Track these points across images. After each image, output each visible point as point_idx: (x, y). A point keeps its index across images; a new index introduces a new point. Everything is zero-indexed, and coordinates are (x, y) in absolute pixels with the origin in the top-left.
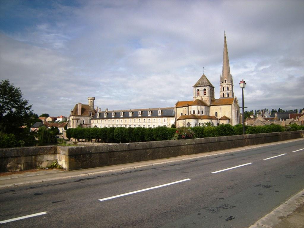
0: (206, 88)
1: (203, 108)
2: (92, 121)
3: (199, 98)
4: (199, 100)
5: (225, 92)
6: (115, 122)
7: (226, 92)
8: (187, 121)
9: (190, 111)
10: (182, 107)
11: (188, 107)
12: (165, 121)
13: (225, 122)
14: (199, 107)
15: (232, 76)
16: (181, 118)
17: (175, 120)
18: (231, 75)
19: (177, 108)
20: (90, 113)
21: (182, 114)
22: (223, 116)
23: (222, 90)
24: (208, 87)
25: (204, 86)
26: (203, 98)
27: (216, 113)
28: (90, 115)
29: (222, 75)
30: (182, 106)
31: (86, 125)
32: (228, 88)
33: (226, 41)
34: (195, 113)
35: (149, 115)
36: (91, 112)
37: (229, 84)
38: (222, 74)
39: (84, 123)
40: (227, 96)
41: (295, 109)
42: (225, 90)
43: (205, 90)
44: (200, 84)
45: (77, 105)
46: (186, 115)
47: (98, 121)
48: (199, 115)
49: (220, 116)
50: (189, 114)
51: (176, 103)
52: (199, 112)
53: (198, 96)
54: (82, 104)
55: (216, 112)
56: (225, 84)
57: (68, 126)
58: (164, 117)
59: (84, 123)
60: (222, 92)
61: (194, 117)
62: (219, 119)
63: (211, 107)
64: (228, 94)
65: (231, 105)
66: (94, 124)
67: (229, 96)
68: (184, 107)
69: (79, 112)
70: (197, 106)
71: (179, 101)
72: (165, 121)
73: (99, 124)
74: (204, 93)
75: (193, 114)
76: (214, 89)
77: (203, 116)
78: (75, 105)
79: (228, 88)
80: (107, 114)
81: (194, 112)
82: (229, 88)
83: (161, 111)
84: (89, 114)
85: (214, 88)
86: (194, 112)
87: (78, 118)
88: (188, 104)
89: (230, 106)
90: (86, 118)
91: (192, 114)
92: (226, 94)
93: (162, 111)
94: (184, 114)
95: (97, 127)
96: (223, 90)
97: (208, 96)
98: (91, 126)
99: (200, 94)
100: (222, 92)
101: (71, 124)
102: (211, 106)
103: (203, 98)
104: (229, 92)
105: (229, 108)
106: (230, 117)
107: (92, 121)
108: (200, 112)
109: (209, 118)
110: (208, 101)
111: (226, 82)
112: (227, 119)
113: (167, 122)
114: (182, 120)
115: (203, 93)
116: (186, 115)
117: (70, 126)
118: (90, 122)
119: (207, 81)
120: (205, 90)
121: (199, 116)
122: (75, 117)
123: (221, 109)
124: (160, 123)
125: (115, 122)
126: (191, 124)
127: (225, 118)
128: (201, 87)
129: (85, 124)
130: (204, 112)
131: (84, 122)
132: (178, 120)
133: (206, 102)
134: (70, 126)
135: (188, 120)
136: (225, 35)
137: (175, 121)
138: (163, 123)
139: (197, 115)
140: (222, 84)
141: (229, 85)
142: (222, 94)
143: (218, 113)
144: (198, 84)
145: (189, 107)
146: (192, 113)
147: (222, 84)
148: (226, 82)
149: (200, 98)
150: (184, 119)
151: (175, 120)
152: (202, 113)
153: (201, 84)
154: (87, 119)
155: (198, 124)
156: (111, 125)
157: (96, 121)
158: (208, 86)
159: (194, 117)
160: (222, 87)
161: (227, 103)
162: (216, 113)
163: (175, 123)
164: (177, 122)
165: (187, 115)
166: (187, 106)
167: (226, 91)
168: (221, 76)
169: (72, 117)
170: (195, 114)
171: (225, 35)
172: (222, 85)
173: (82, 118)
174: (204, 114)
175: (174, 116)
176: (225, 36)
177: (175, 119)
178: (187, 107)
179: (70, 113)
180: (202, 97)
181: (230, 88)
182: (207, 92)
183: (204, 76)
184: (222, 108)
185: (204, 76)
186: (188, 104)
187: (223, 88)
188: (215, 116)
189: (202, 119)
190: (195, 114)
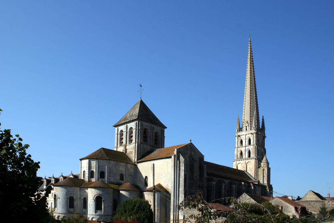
5: (243, 149)
14: (94, 163)
32: (250, 140)
52: (91, 174)
67: (251, 155)
75: (83, 178)
76: (165, 130)
79: (250, 140)
82: (252, 141)
102: (138, 163)
104: (252, 147)
105: (168, 166)
108: (96, 175)
111: (246, 129)
140: (240, 133)
141: (252, 134)
148: (246, 129)
172: (239, 136)
181: (253, 141)
187: (241, 142)
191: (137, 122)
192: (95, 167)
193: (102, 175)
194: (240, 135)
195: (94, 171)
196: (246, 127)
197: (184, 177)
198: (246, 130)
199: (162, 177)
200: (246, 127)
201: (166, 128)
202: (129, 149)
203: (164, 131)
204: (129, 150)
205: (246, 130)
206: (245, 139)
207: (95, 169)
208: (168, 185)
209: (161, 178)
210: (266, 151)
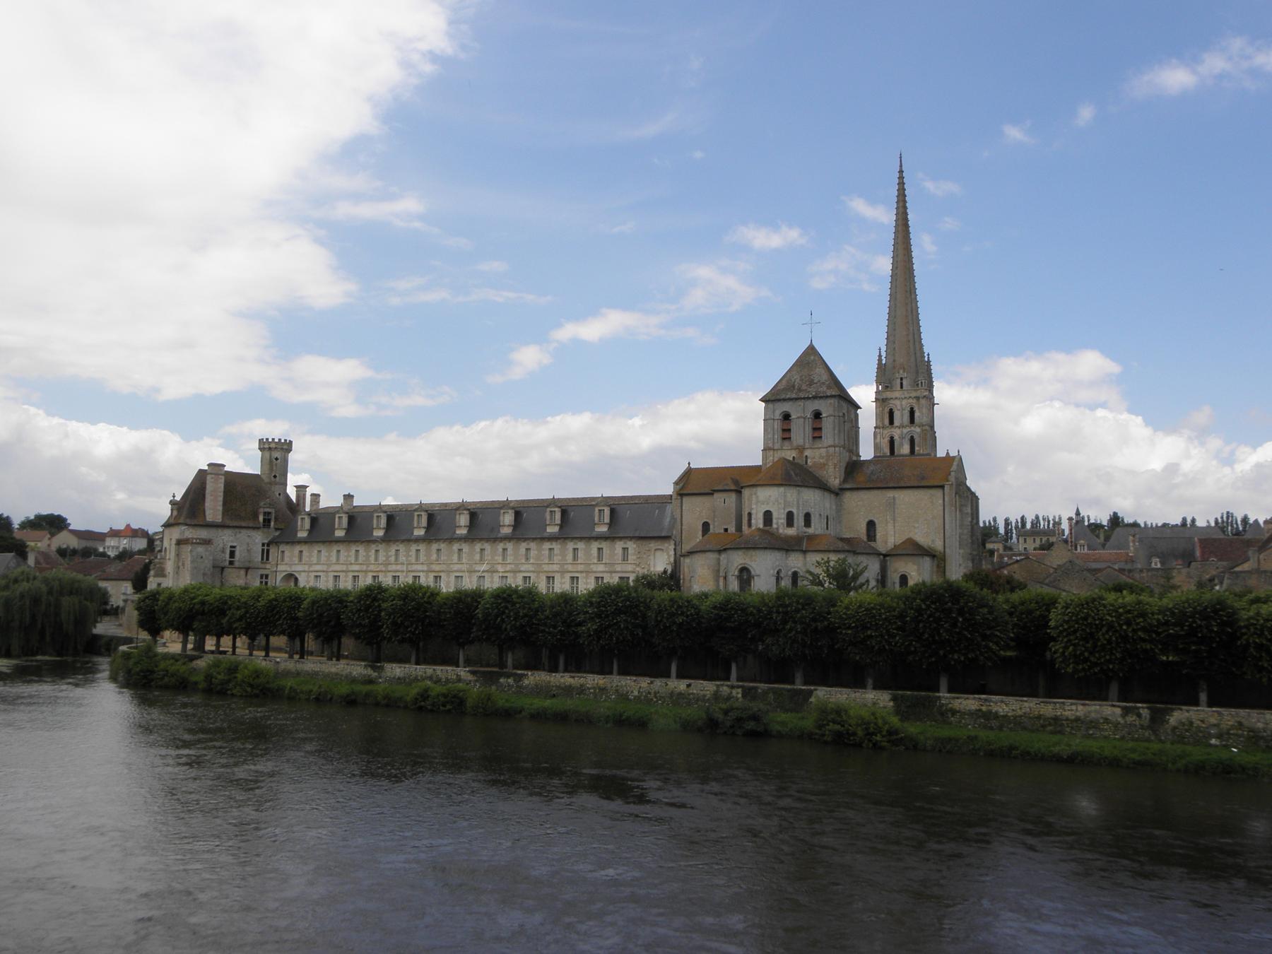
0: (826, 408)
1: (811, 499)
2: (273, 550)
3: (790, 455)
4: (789, 461)
5: (896, 433)
6: (388, 557)
7: (905, 431)
8: (737, 560)
9: (750, 514)
10: (711, 494)
11: (739, 492)
12: (625, 558)
13: (918, 573)
14: (791, 494)
15: (929, 361)
16: (708, 547)
17: (672, 553)
18: (925, 355)
19: (685, 499)
20: (265, 513)
21: (706, 527)
22: (907, 537)
23: (887, 422)
24: (831, 401)
25: (815, 397)
26: (807, 453)
27: (871, 525)
28: (267, 522)
29: (884, 354)
30: (707, 491)
31: (243, 572)
32: (912, 412)
33: (905, 202)
34: (774, 521)
35: (553, 530)
36: (272, 511)
37: (918, 394)
38: (884, 349)
39: (231, 563)
40: (906, 449)
41: (1216, 519)
42: (897, 423)
43: (817, 415)
44: (793, 386)
45: (201, 475)
46: (726, 530)
47: (305, 554)
48: (791, 532)
49: (889, 537)
50: (745, 527)
51: (676, 477)
52: (790, 518)
53: (786, 443)
54: (226, 469)
55: (872, 519)
56: (897, 394)
57: (152, 573)
58: (621, 538)
59: (231, 563)
60: (887, 432)
61: (771, 541)
62: (885, 556)
63: (848, 495)
64: (912, 441)
65: (942, 487)
66: (281, 568)
67: (917, 448)
68: (716, 495)
69: (213, 508)
70: (782, 489)
71: (692, 466)
72: (625, 558)
73: (306, 568)
74: (815, 429)
75: (765, 524)
76: (859, 411)
77: (811, 538)
78: (189, 478)
79: (912, 412)
80: (351, 519)
81: (768, 516)
82: (917, 414)
83: (607, 511)
84: (261, 518)
85: (859, 407)
86: (768, 516)
87: (203, 534)
88: (736, 482)
89: (938, 493)
90: (244, 534)
91: (761, 526)
92: (902, 438)
93: (613, 512)
94: (716, 529)
95: (296, 579)
96: (891, 422)
97: (830, 442)
98: (267, 576)
99: (793, 435)
100: (887, 432)
101: (169, 567)
103: (807, 453)
104: (918, 430)
106: (938, 545)
107: (273, 550)
108: (799, 521)
109: (840, 545)
110: (831, 469)
111: (902, 384)
112: (922, 555)
113: (638, 565)
114: (715, 556)
115: (808, 430)
116: (726, 530)
117: (164, 576)
118: (266, 555)
119: (825, 377)
120: (817, 415)
121: (791, 537)
122: (189, 533)
123: (892, 505)
124: (601, 568)
125: (388, 557)
126: (753, 573)
127: (914, 550)
128: (801, 403)
129: (237, 564)
130: (814, 520)
131: (232, 554)
132: (690, 553)
133: (821, 474)
134: (161, 573)
135: (740, 553)
136: (901, 172)
137: (675, 561)
138: (618, 568)
139: (781, 531)
140: (888, 394)
141: (918, 398)
142: (887, 440)
143: (877, 526)
144: (786, 390)
145: (746, 492)
146: (758, 522)
147: (888, 394)
148: (902, 384)
149: (794, 454)
150: (720, 552)
151: (675, 554)
152: (808, 519)
153: (800, 390)
154: (250, 542)
155: (790, 573)
156: (366, 572)
157: (291, 553)
158: (832, 396)
159: (771, 541)
160: (887, 410)
161: (923, 478)
162: (871, 525)
163: (676, 565)
164: (687, 561)
165: (732, 529)
166: (733, 488)
167: (902, 426)
168: (880, 356)
169: (176, 533)
170: (771, 525)
171: (901, 172)
173: (226, 538)
174: (811, 531)
175: (667, 538)
176: (901, 178)
177: (675, 549)
178: (733, 496)
179: (165, 512)
180: (801, 449)
182: (828, 425)
183: (811, 350)
184: (897, 501)
185: (811, 350)
186: (736, 482)
188: (865, 540)
189: (805, 552)
190: (775, 526)
191: (836, 401)
192: (795, 503)
193: (808, 519)
194: (889, 397)
195: (795, 511)
196: (902, 379)
197: (970, 527)
198: (902, 387)
199: (917, 525)
200: (902, 379)
201: (861, 408)
202: (814, 458)
203: (858, 415)
204: (814, 460)
205: (902, 387)
206: (899, 408)
207: (795, 508)
208: (933, 541)
209: (915, 527)
210: (936, 437)
